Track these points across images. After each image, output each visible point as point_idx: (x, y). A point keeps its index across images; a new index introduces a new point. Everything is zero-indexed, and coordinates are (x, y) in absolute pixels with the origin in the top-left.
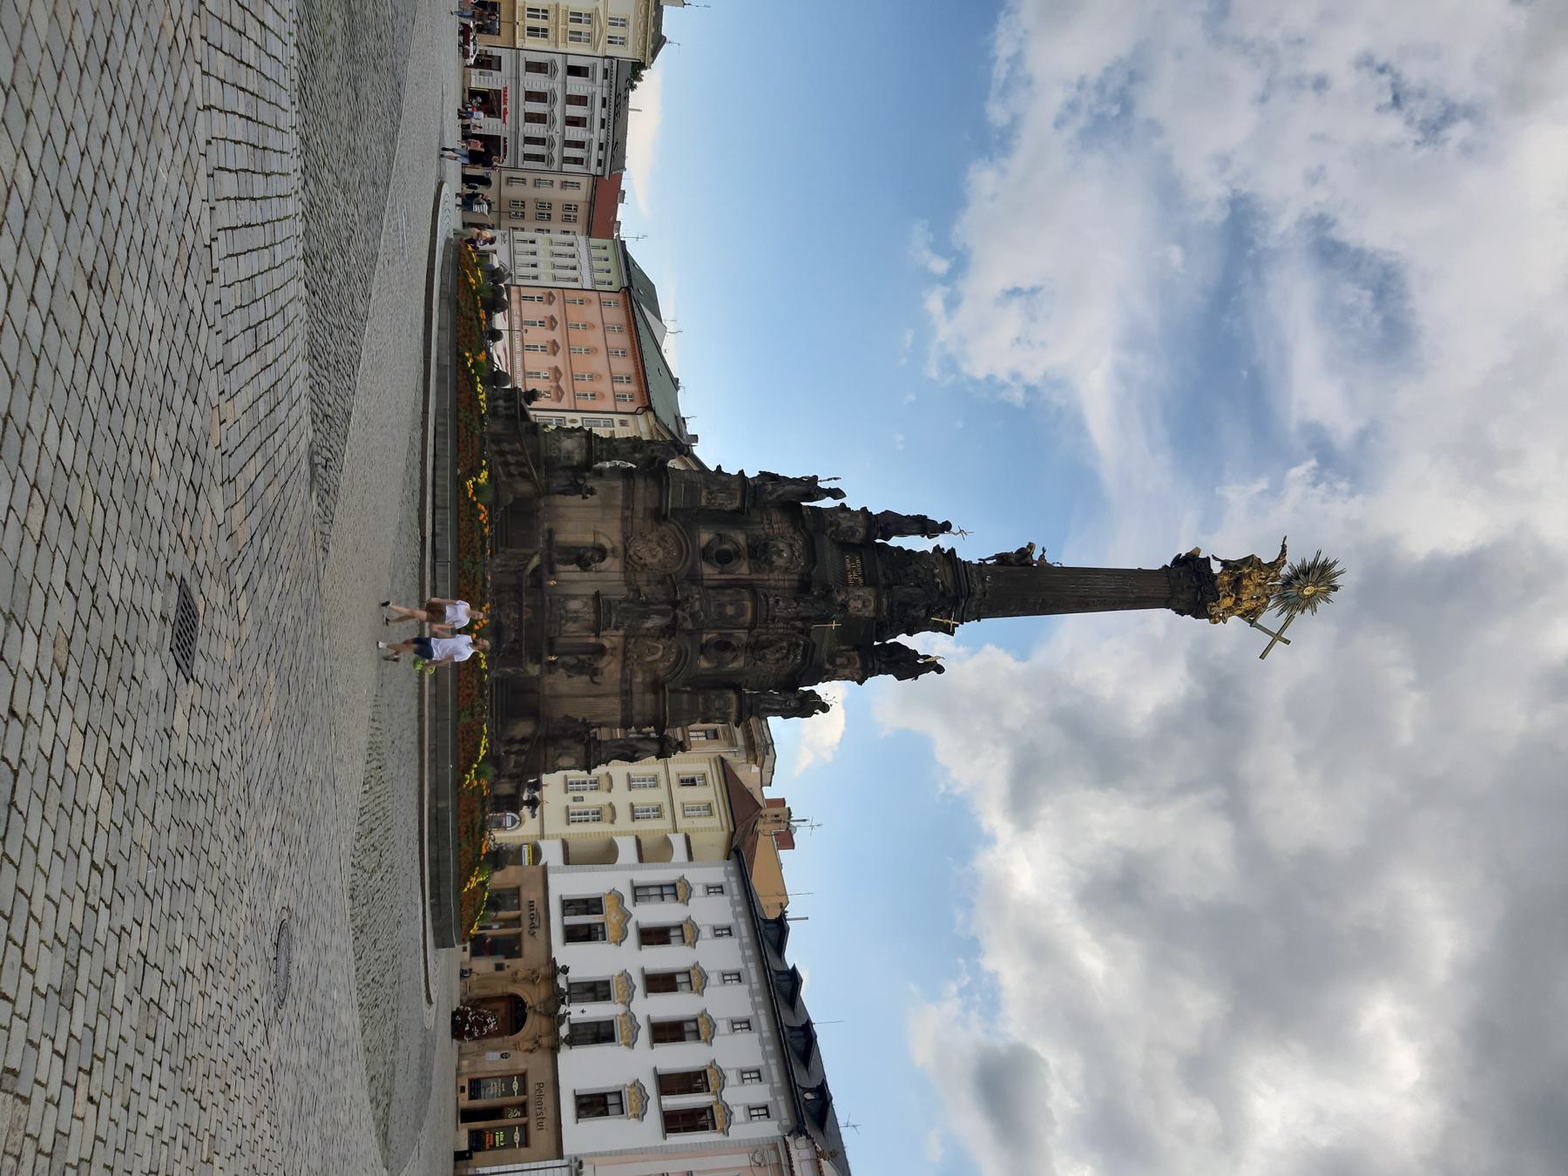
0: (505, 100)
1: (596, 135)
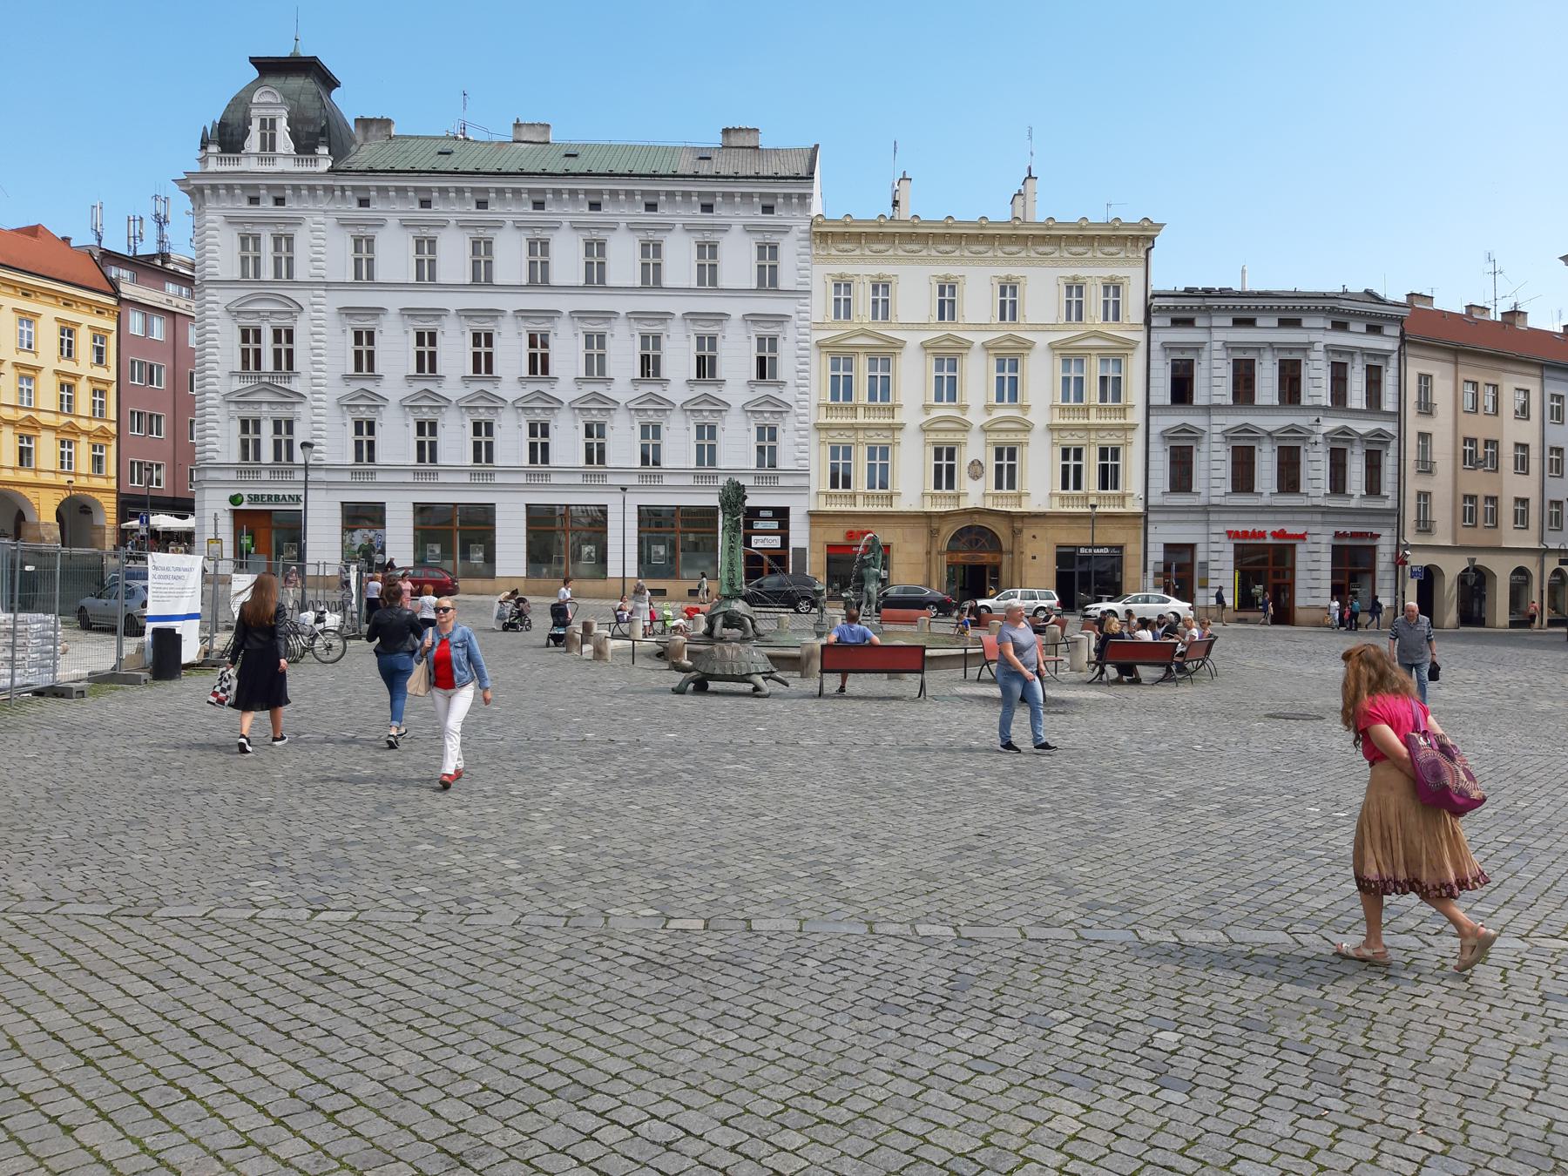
0: (1254, 535)
1: (1318, 336)
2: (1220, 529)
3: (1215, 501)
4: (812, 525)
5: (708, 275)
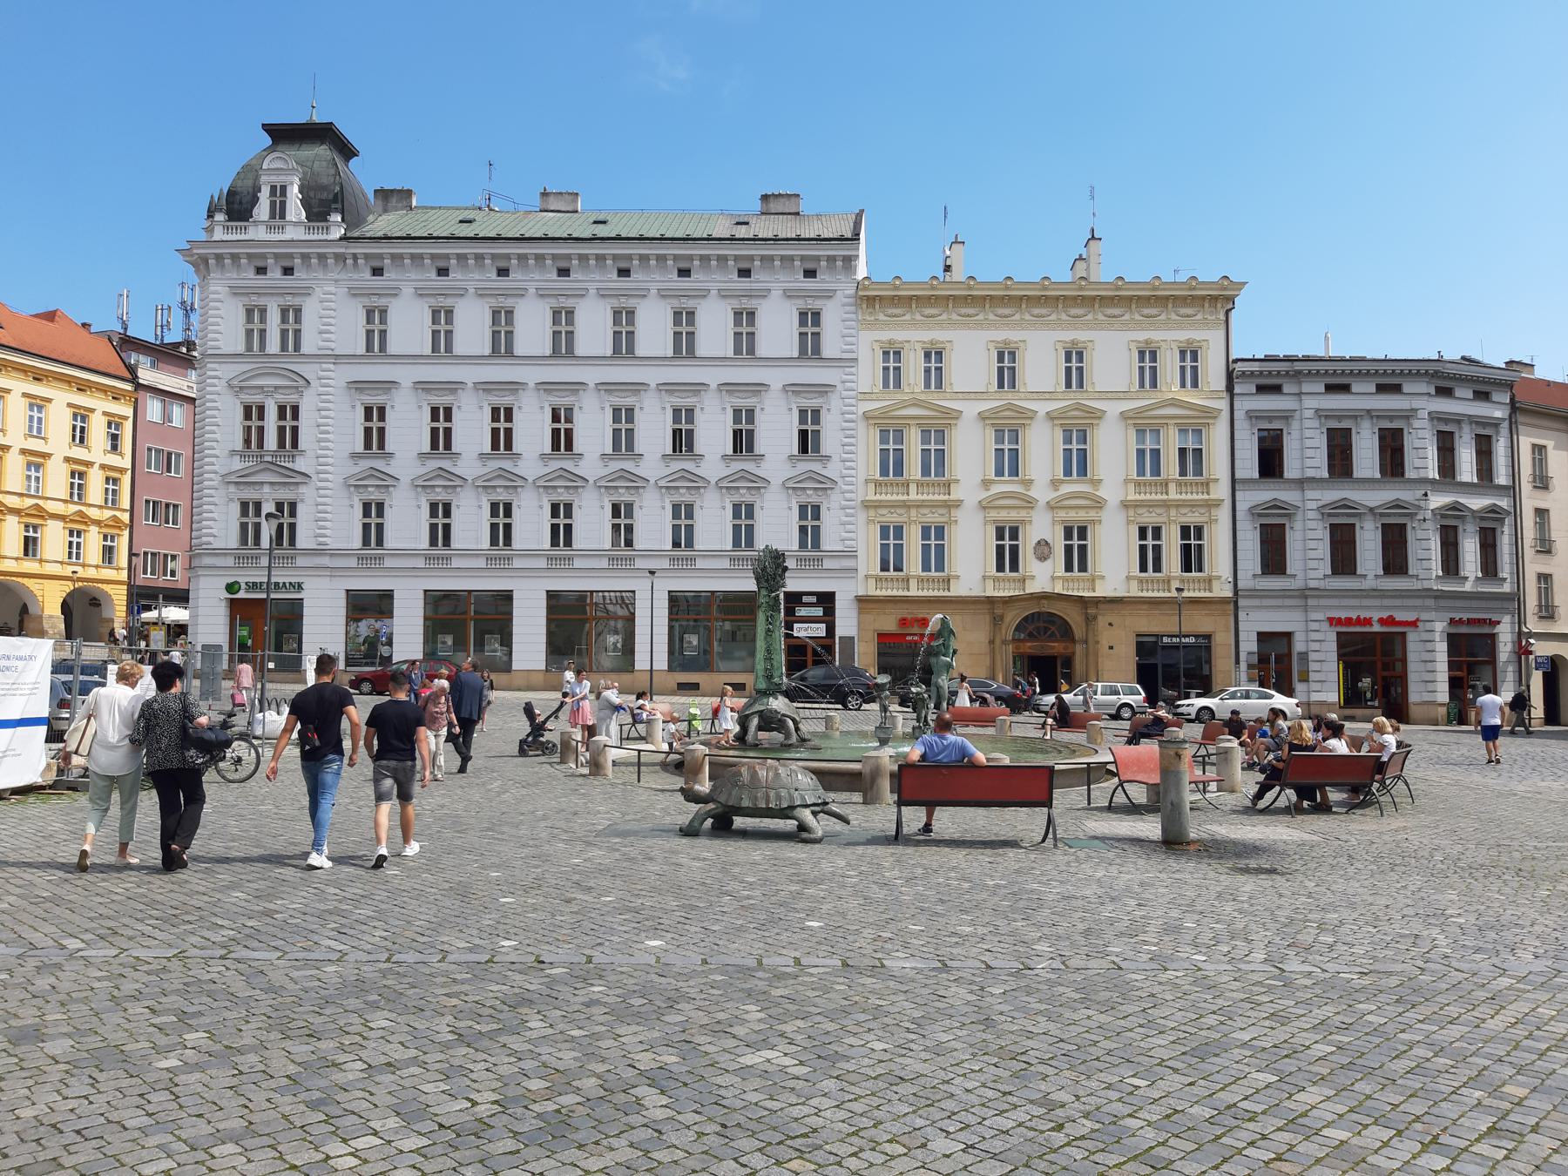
0: (1359, 622)
1: (1422, 403)
2: (1320, 616)
3: (1312, 584)
4: (861, 611)
5: (745, 345)
